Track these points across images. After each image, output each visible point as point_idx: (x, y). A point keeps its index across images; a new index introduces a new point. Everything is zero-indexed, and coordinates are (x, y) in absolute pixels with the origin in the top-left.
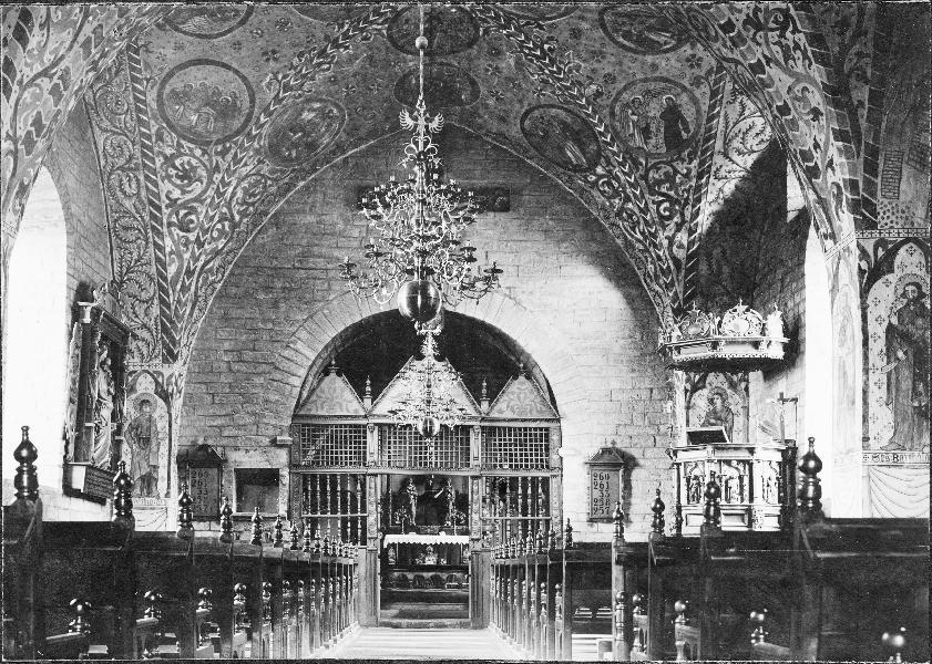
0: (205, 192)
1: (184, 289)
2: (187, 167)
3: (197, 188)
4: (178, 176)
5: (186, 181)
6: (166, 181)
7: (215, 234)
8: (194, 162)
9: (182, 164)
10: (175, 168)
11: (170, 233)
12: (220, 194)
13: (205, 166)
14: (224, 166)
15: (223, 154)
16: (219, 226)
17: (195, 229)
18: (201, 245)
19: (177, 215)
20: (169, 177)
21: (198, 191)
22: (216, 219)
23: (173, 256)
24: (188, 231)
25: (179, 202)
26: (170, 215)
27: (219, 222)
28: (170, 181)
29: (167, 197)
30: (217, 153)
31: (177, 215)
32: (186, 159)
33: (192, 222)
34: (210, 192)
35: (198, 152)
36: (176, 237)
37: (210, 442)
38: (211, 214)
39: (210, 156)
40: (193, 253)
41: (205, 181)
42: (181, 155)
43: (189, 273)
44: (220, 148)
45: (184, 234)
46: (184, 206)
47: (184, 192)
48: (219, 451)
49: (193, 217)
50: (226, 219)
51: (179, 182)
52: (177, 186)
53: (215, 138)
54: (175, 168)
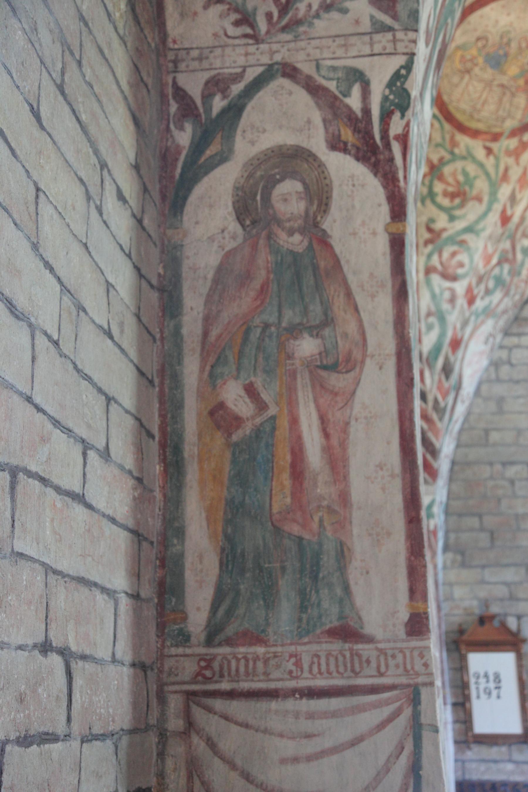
0: (485, 215)
1: (447, 370)
2: (461, 178)
3: (471, 212)
4: (445, 194)
5: (457, 201)
6: (428, 202)
7: (491, 284)
8: (471, 169)
9: (454, 174)
10: (441, 178)
11: (428, 283)
12: (505, 219)
13: (487, 174)
14: (515, 173)
15: (516, 154)
16: (497, 271)
17: (464, 276)
18: (471, 301)
19: (440, 256)
20: (431, 195)
21: (471, 217)
22: (494, 261)
23: (431, 319)
24: (454, 278)
25: (445, 235)
26: (429, 256)
27: (499, 263)
28: (434, 202)
29: (429, 230)
30: (509, 153)
31: (440, 256)
32: (459, 165)
33: (461, 265)
34: (494, 217)
35: (480, 153)
36: (437, 290)
37: (495, 609)
38: (490, 250)
39: (497, 158)
40: (462, 312)
41: (486, 199)
42: (454, 157)
43: (456, 344)
44: (513, 143)
45: (447, 284)
46: (452, 240)
47: (452, 218)
48: (512, 623)
49: (463, 257)
50: (507, 260)
51: (446, 202)
52: (440, 207)
53: (510, 124)
54: (441, 178)
